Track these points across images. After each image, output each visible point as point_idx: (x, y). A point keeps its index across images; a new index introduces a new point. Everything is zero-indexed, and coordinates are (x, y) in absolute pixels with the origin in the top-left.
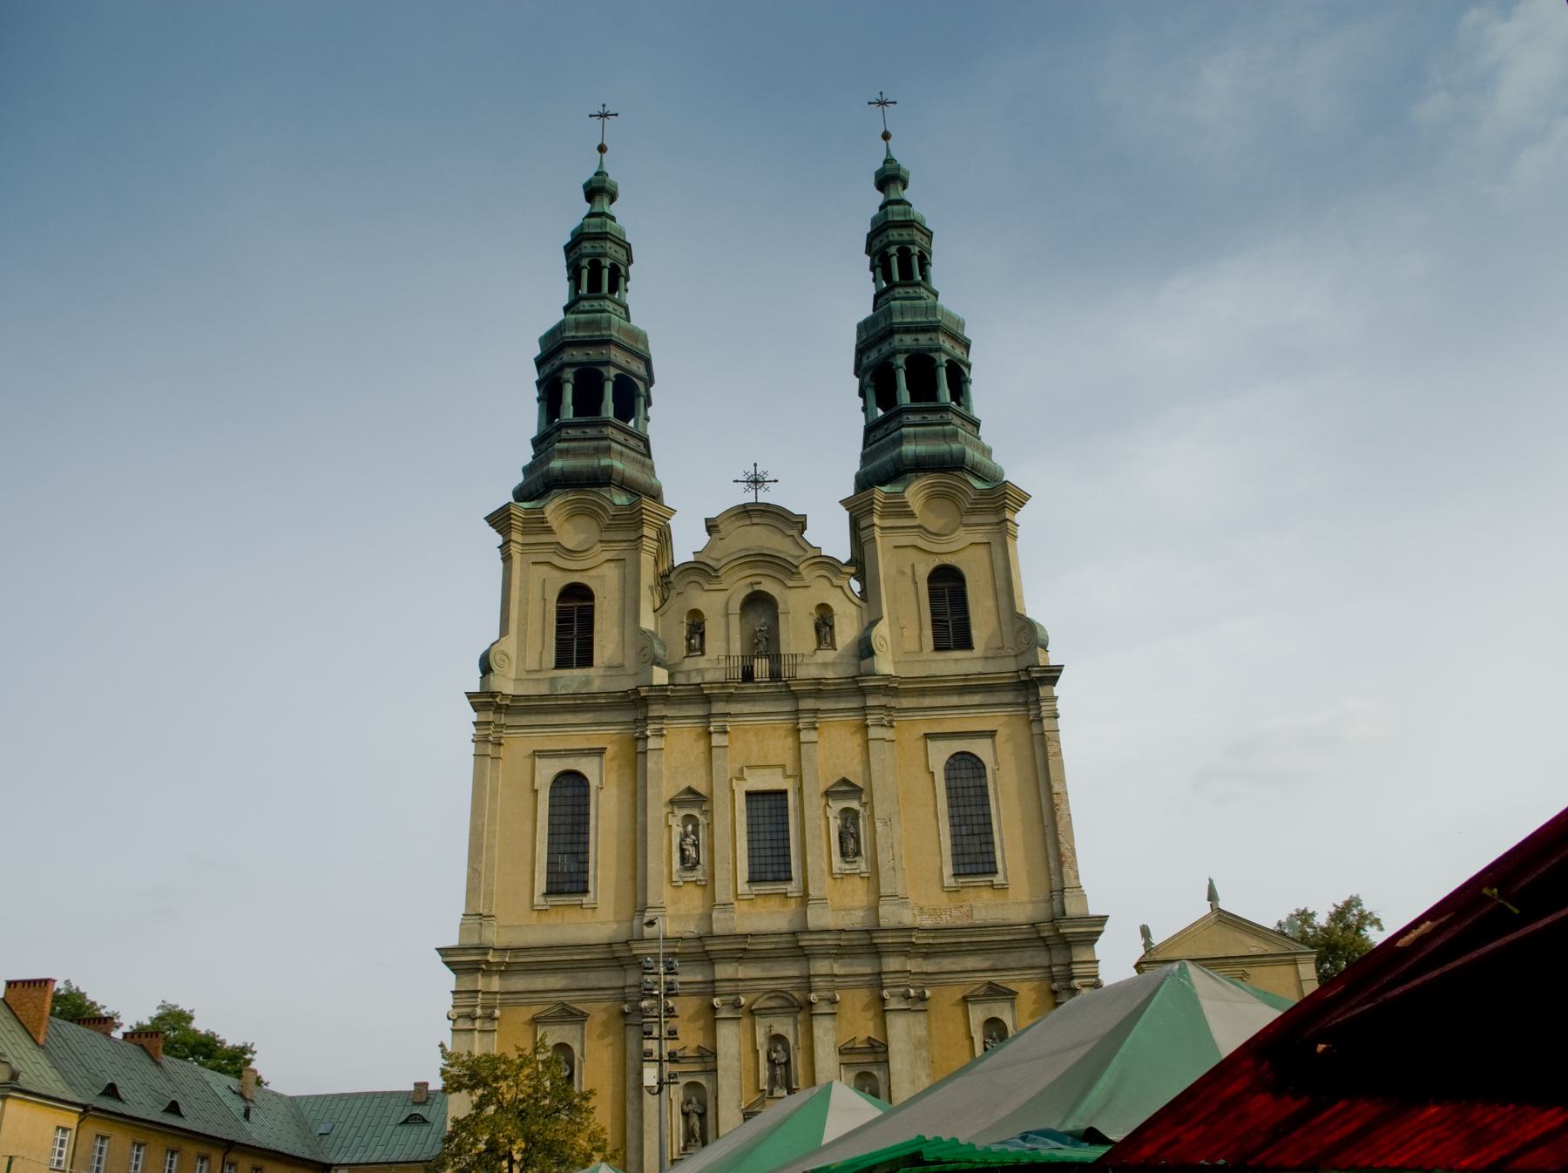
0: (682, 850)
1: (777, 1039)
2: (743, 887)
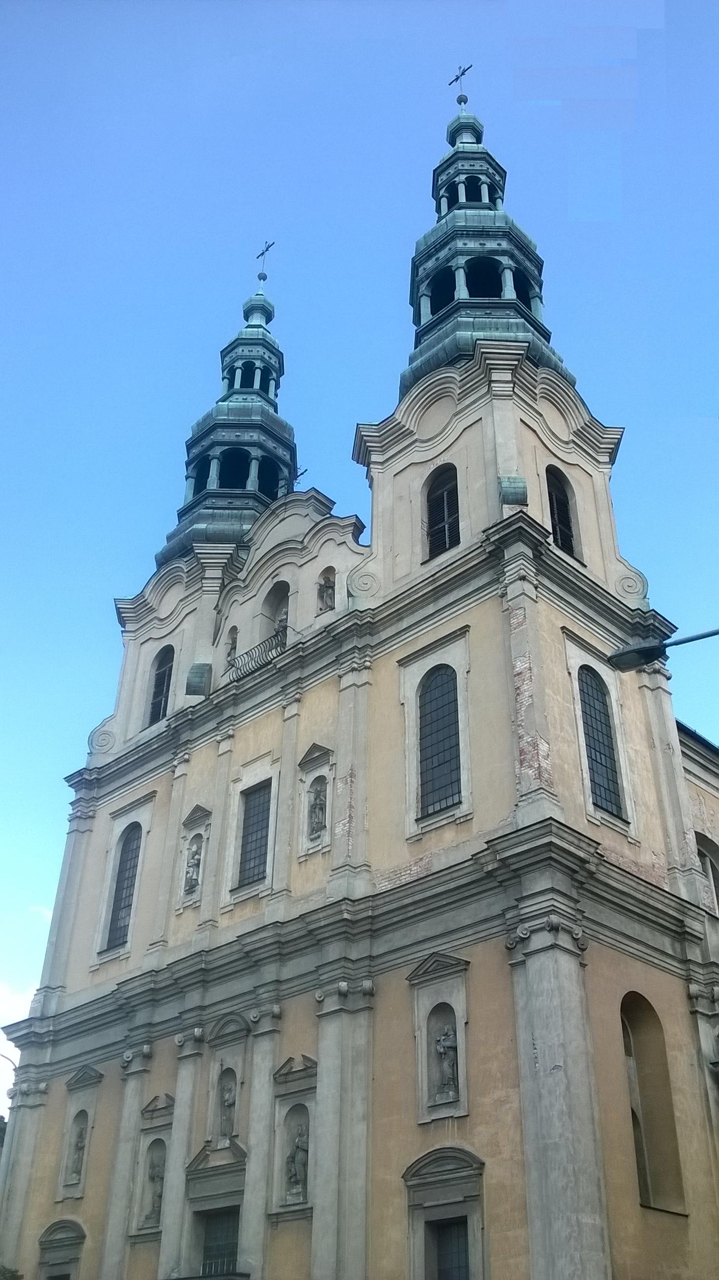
2: (226, 898)
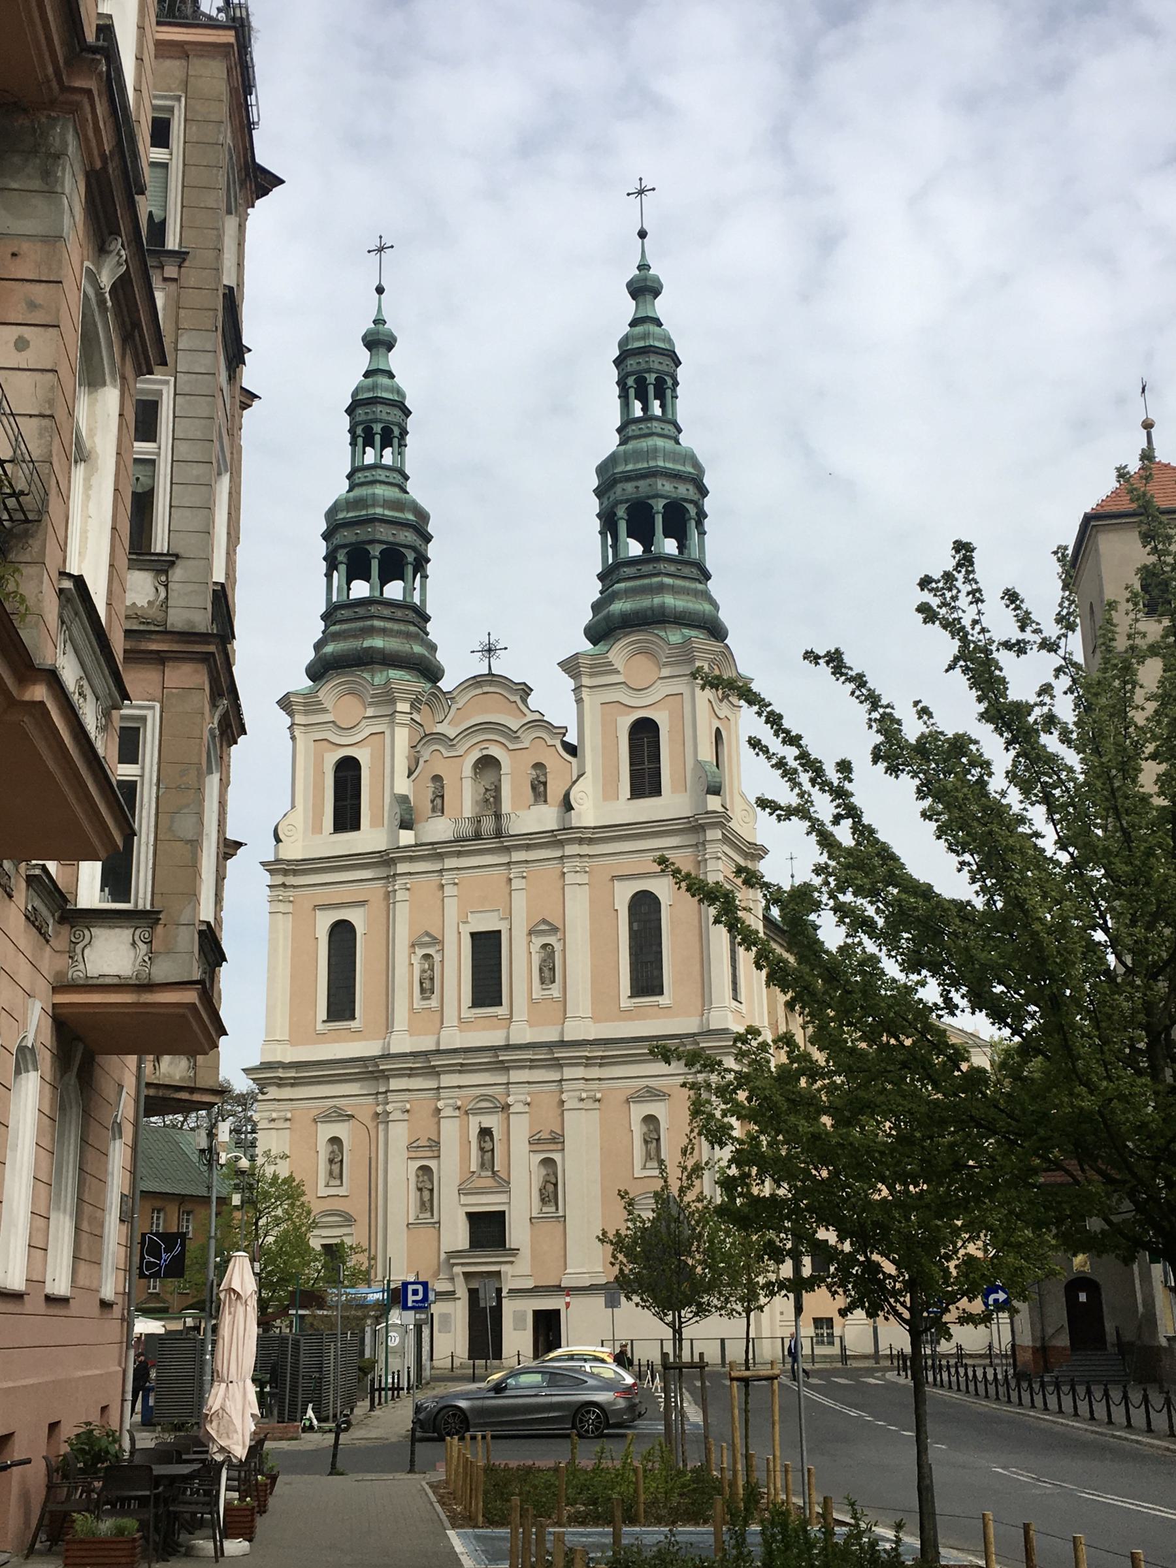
0: (421, 983)
1: (485, 1133)
